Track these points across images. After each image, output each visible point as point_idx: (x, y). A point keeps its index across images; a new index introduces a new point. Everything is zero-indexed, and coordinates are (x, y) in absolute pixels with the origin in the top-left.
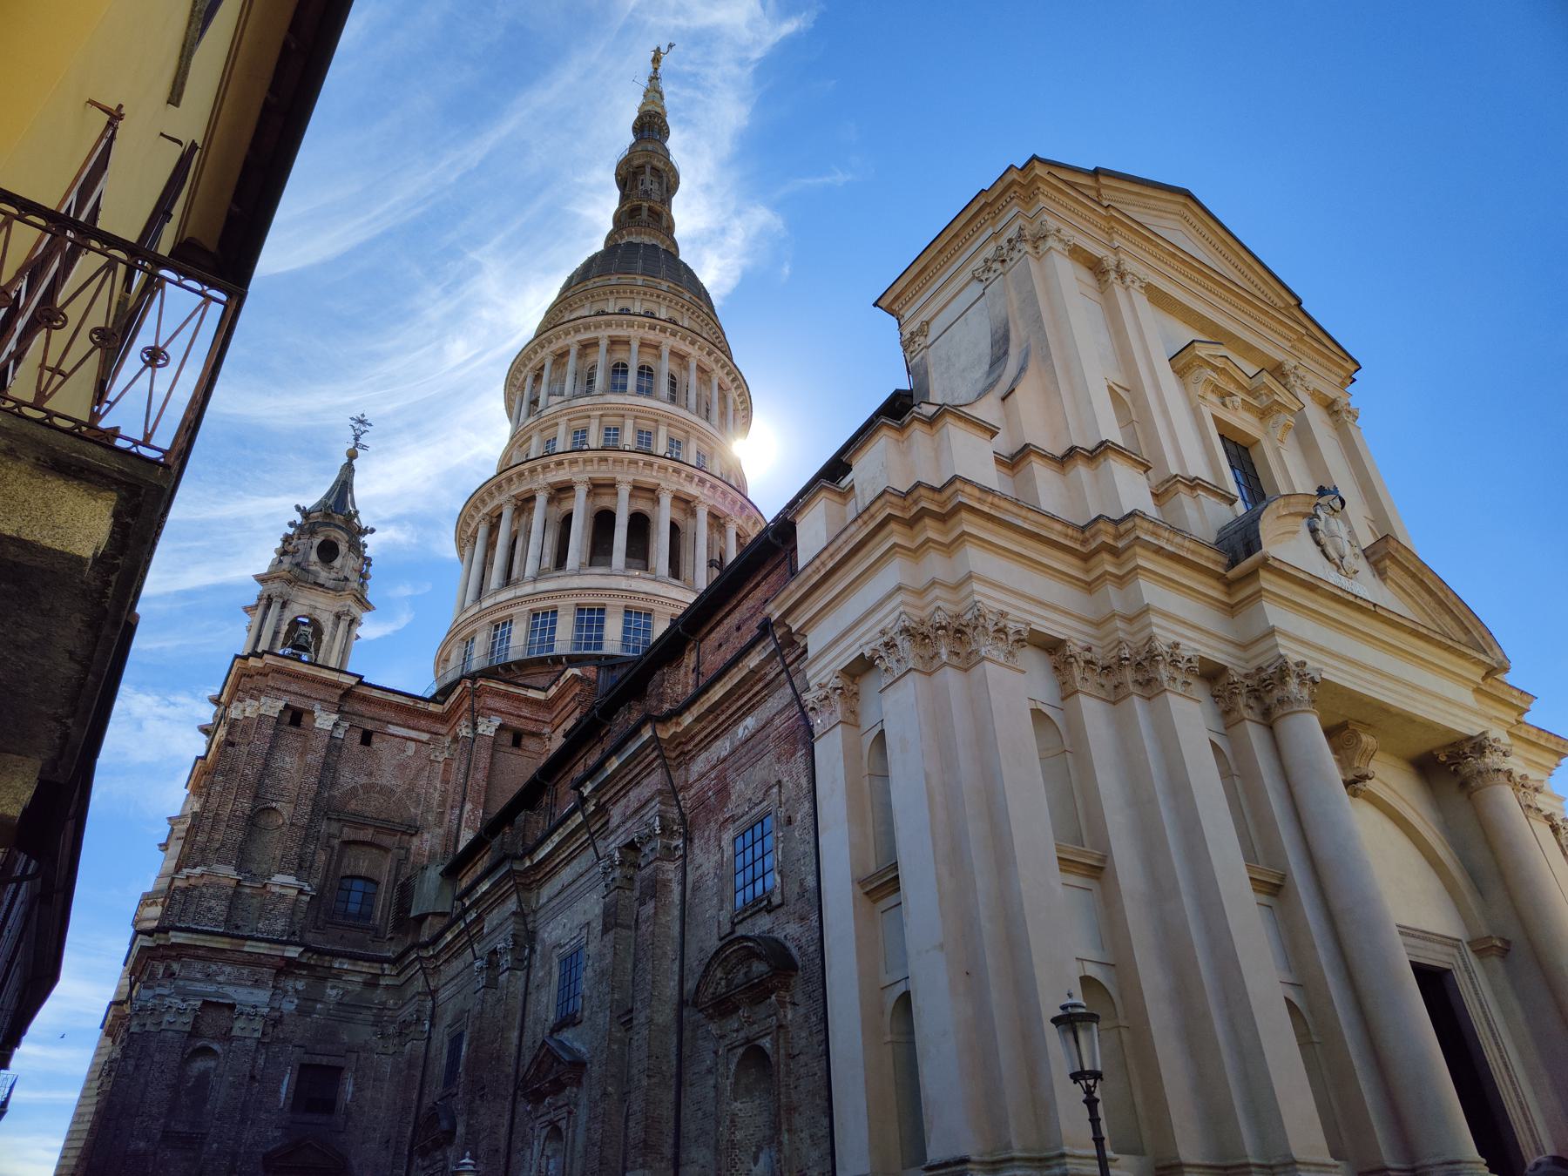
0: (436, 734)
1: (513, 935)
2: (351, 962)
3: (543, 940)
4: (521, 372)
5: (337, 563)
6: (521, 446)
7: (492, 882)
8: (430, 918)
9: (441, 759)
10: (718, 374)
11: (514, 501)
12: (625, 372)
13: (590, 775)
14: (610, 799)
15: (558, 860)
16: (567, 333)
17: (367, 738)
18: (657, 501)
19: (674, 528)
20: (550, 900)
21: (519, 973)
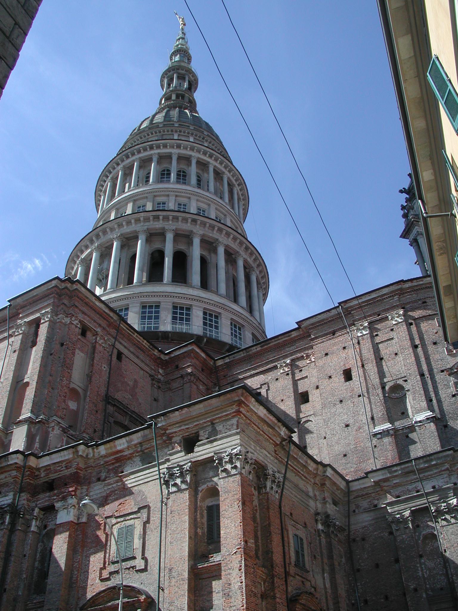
10: (227, 175)
12: (169, 174)
18: (190, 243)
19: (203, 261)
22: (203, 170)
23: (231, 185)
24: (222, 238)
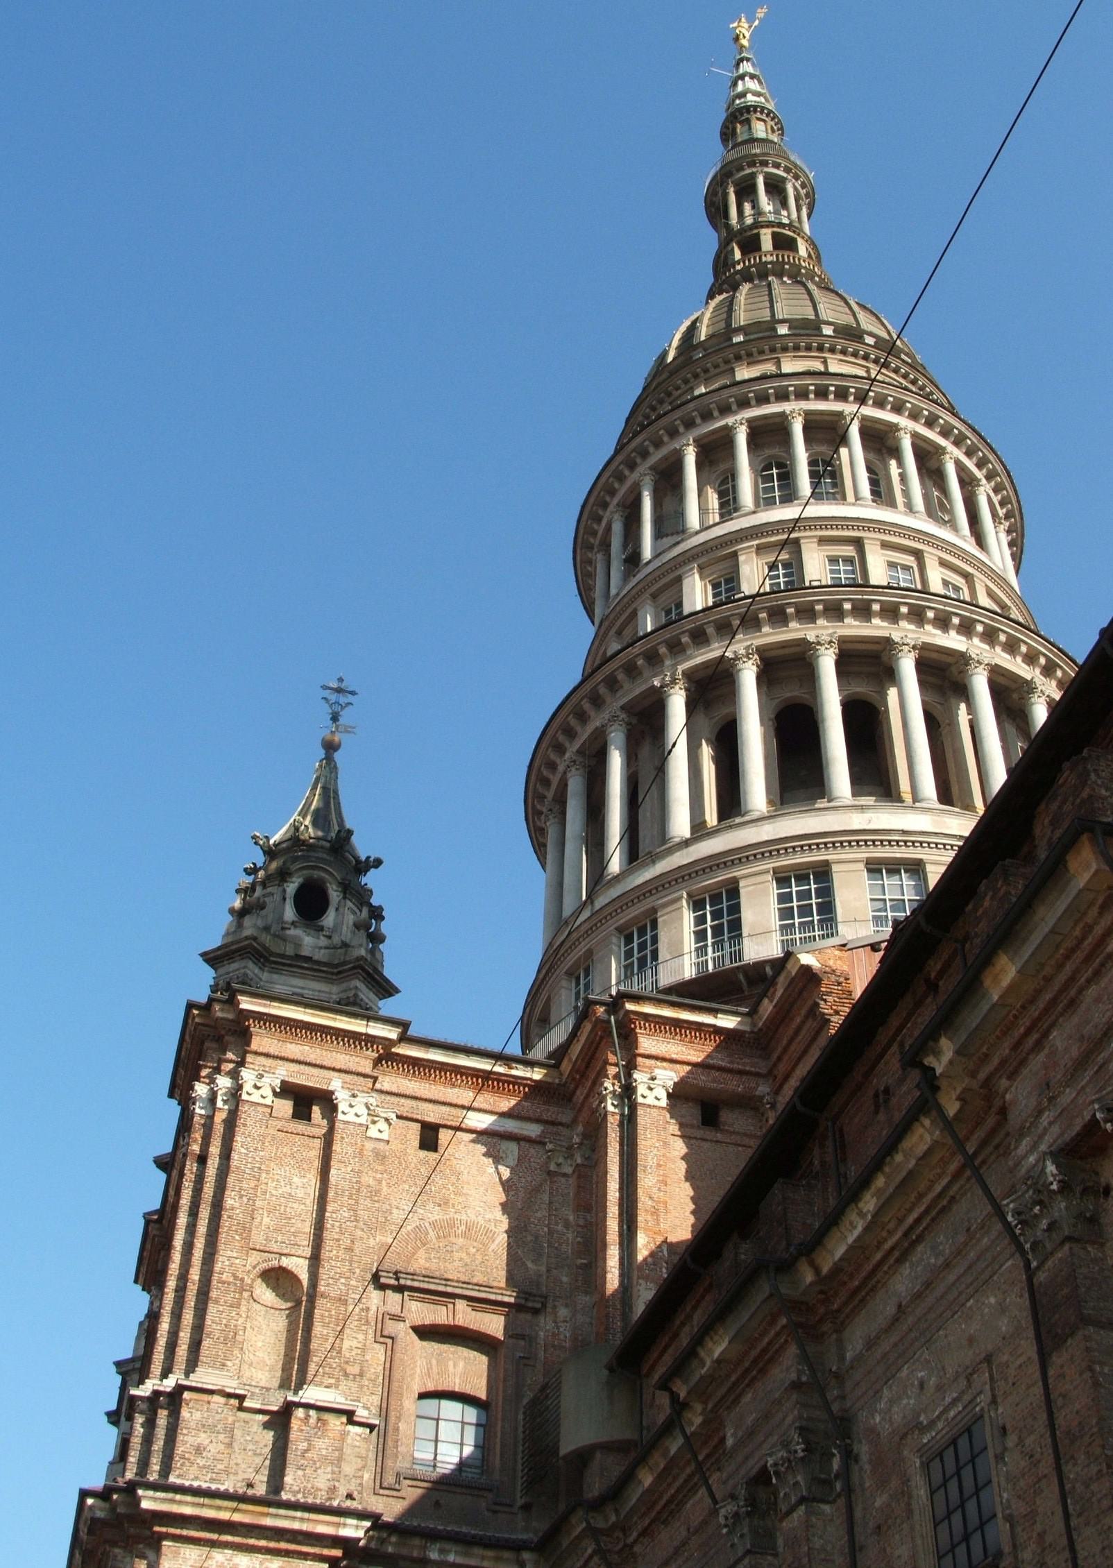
0: (553, 1123)
1: (802, 1430)
2: (459, 1548)
3: (872, 1431)
4: (599, 519)
5: (329, 919)
6: (619, 633)
7: (732, 1333)
8: (598, 1455)
9: (569, 1170)
11: (623, 716)
13: (944, 1023)
14: (1003, 1063)
15: (878, 1256)
17: (429, 1137)
20: (871, 1344)
21: (826, 1508)
22: (879, 451)
23: (967, 479)
24: (975, 647)
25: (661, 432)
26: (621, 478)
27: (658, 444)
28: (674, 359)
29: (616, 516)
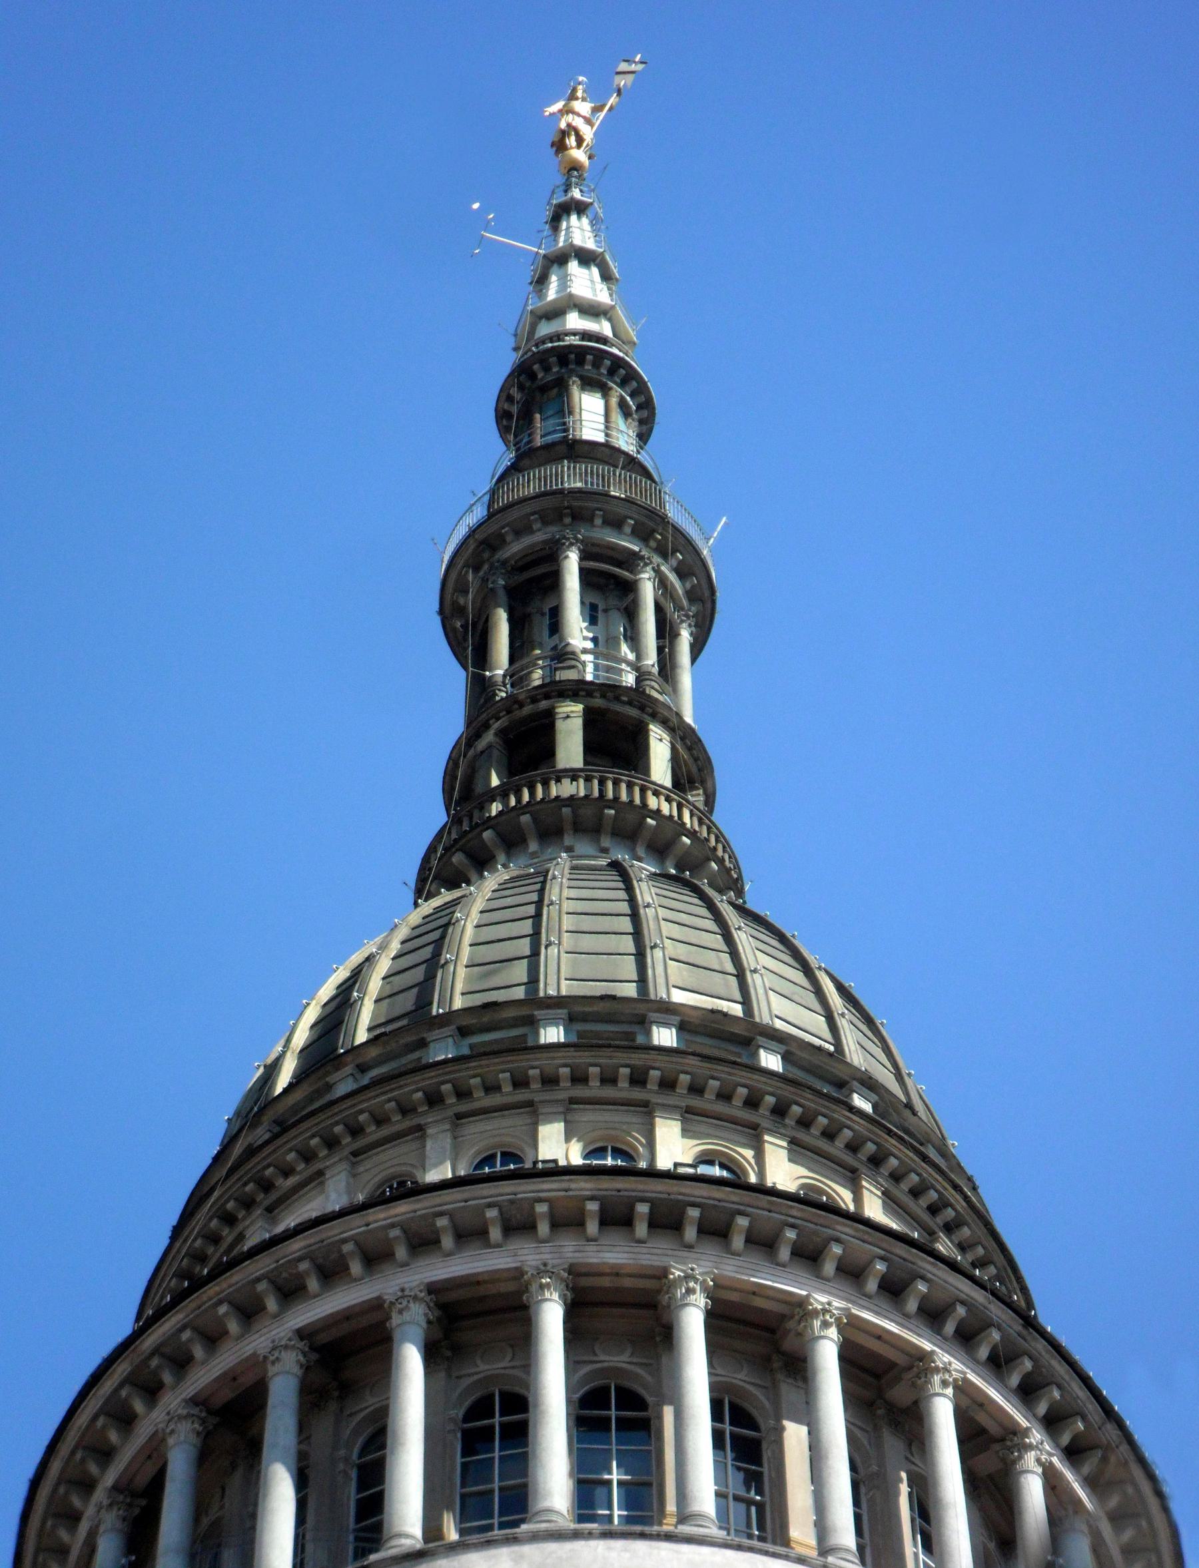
4: (72, 1518)
16: (249, 1312)
25: (223, 1309)
26: (126, 1420)
27: (213, 1339)
28: (286, 1091)
29: (110, 1519)
